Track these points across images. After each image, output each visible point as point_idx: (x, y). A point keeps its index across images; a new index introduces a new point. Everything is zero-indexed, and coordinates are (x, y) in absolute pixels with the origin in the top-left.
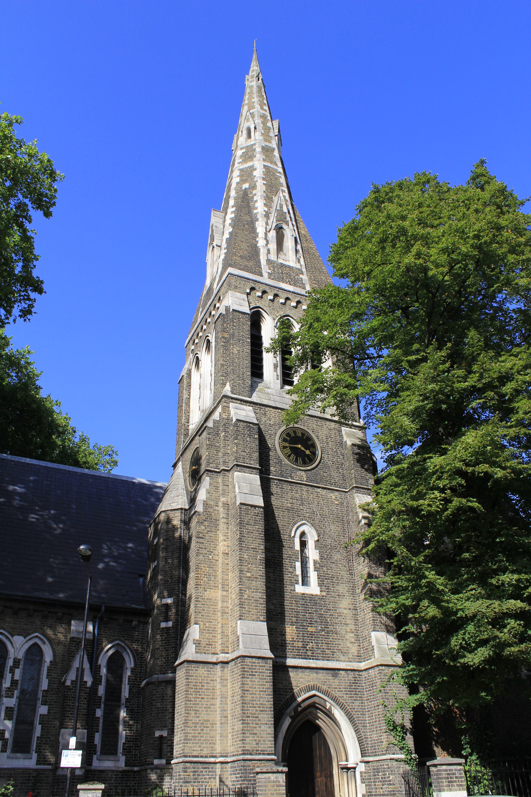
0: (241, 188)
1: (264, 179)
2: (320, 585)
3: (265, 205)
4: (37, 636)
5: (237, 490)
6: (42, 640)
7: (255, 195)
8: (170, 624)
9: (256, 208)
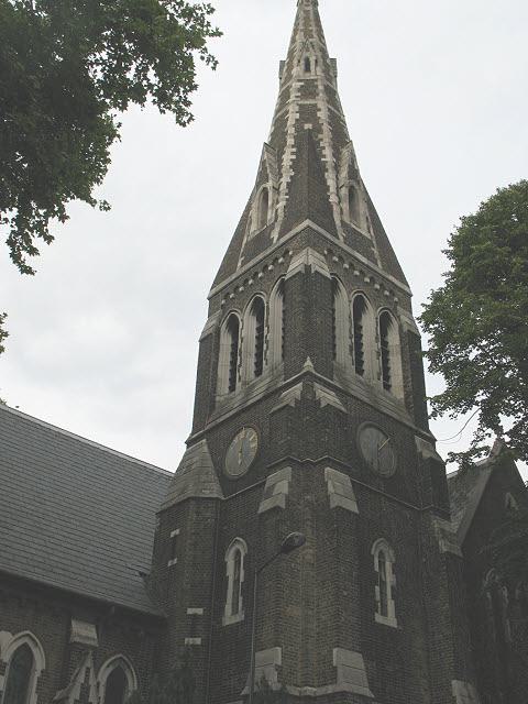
0: (303, 127)
1: (330, 124)
2: (397, 616)
3: (334, 155)
4: (28, 635)
5: (331, 489)
6: (33, 640)
7: (322, 140)
8: (198, 641)
9: (324, 156)
